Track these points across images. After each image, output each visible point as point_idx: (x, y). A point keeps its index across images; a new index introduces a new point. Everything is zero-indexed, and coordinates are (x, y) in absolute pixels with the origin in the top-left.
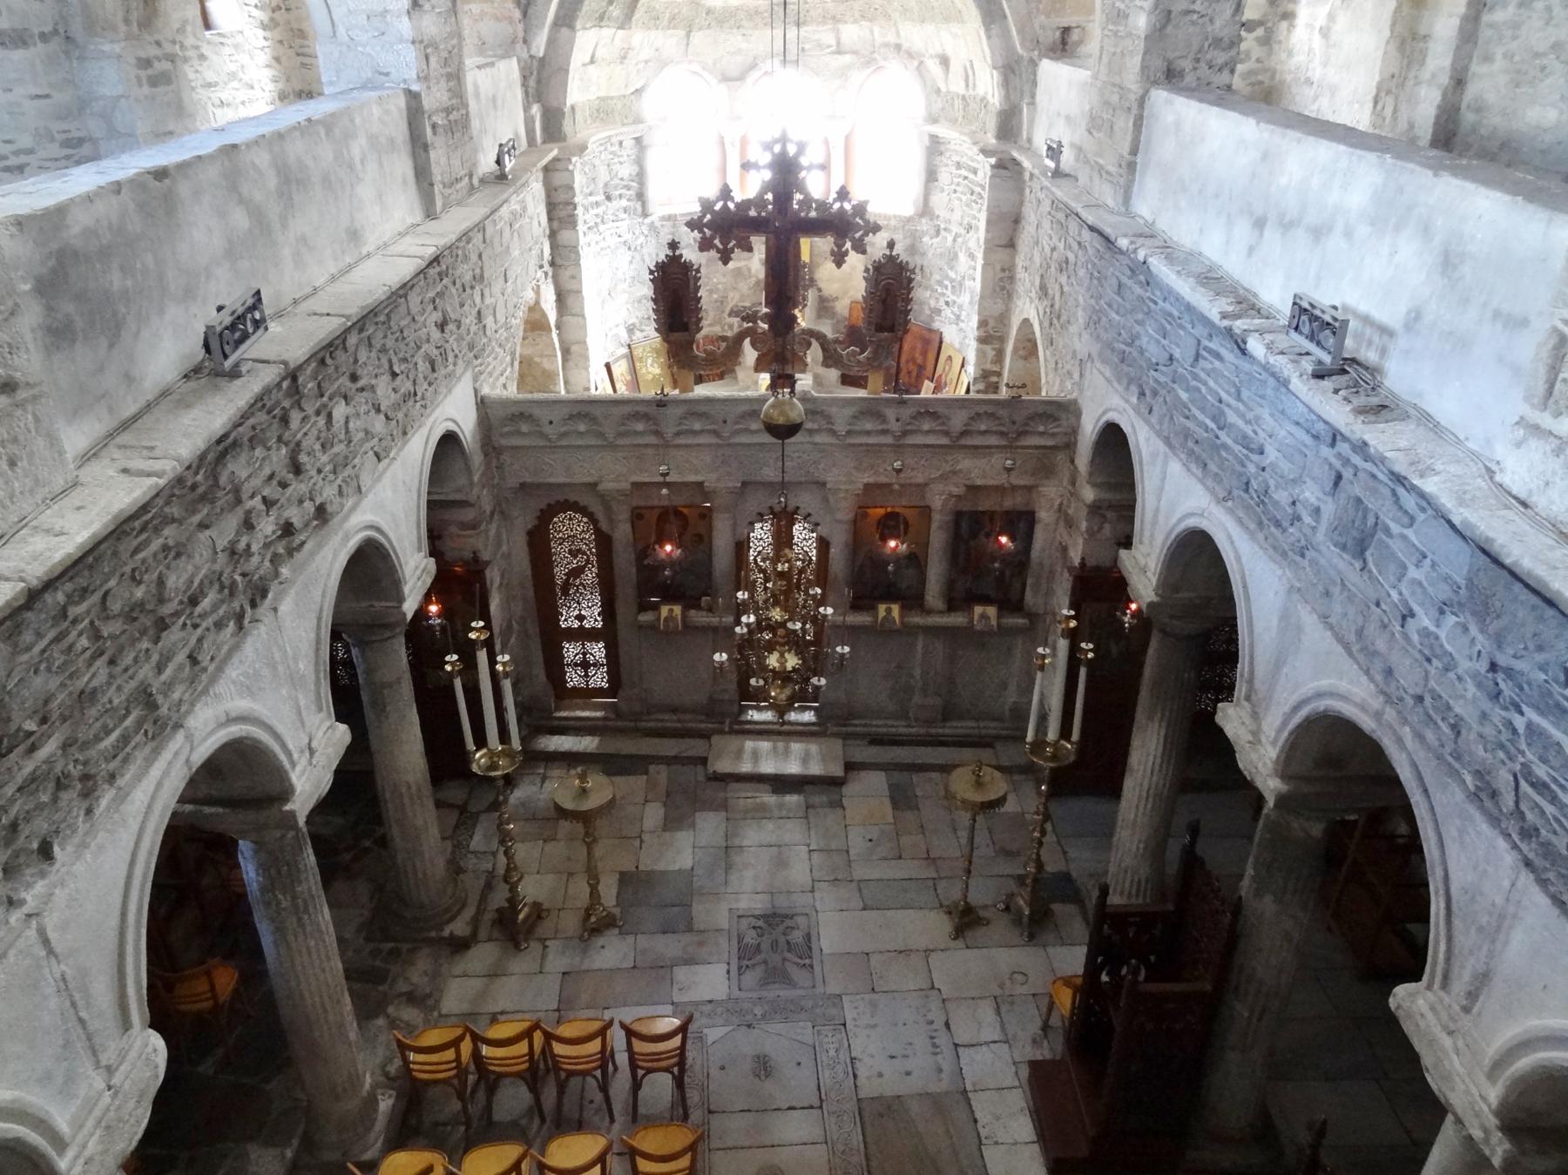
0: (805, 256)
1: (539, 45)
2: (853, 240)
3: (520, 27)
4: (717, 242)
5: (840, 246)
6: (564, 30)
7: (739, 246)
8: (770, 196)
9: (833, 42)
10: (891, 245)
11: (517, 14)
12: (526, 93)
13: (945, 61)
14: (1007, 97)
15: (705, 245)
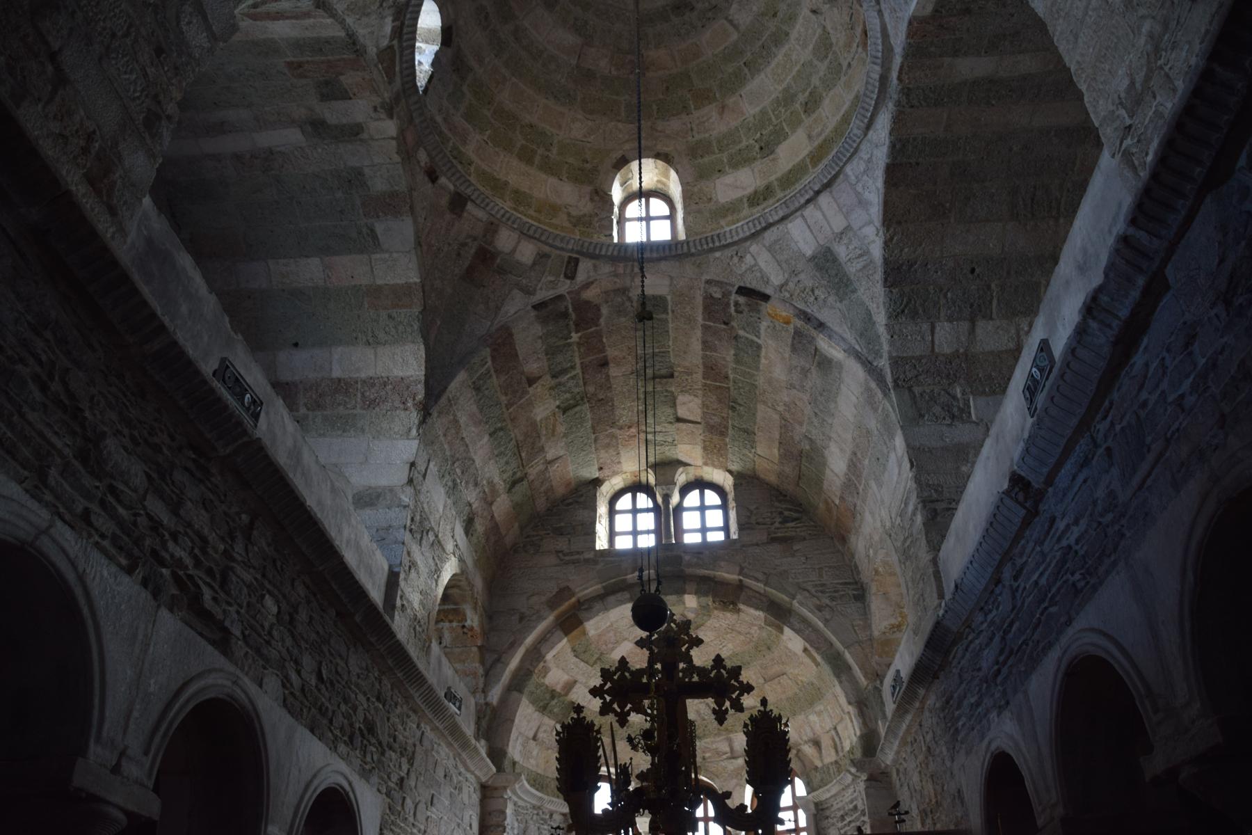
0: (691, 715)
1: (495, 695)
2: (731, 699)
3: (481, 681)
4: (615, 706)
5: (720, 704)
6: (515, 694)
7: (634, 709)
8: (659, 666)
9: (728, 749)
10: (764, 702)
11: (481, 671)
12: (478, 729)
13: (817, 744)
14: (865, 724)
15: (605, 710)
